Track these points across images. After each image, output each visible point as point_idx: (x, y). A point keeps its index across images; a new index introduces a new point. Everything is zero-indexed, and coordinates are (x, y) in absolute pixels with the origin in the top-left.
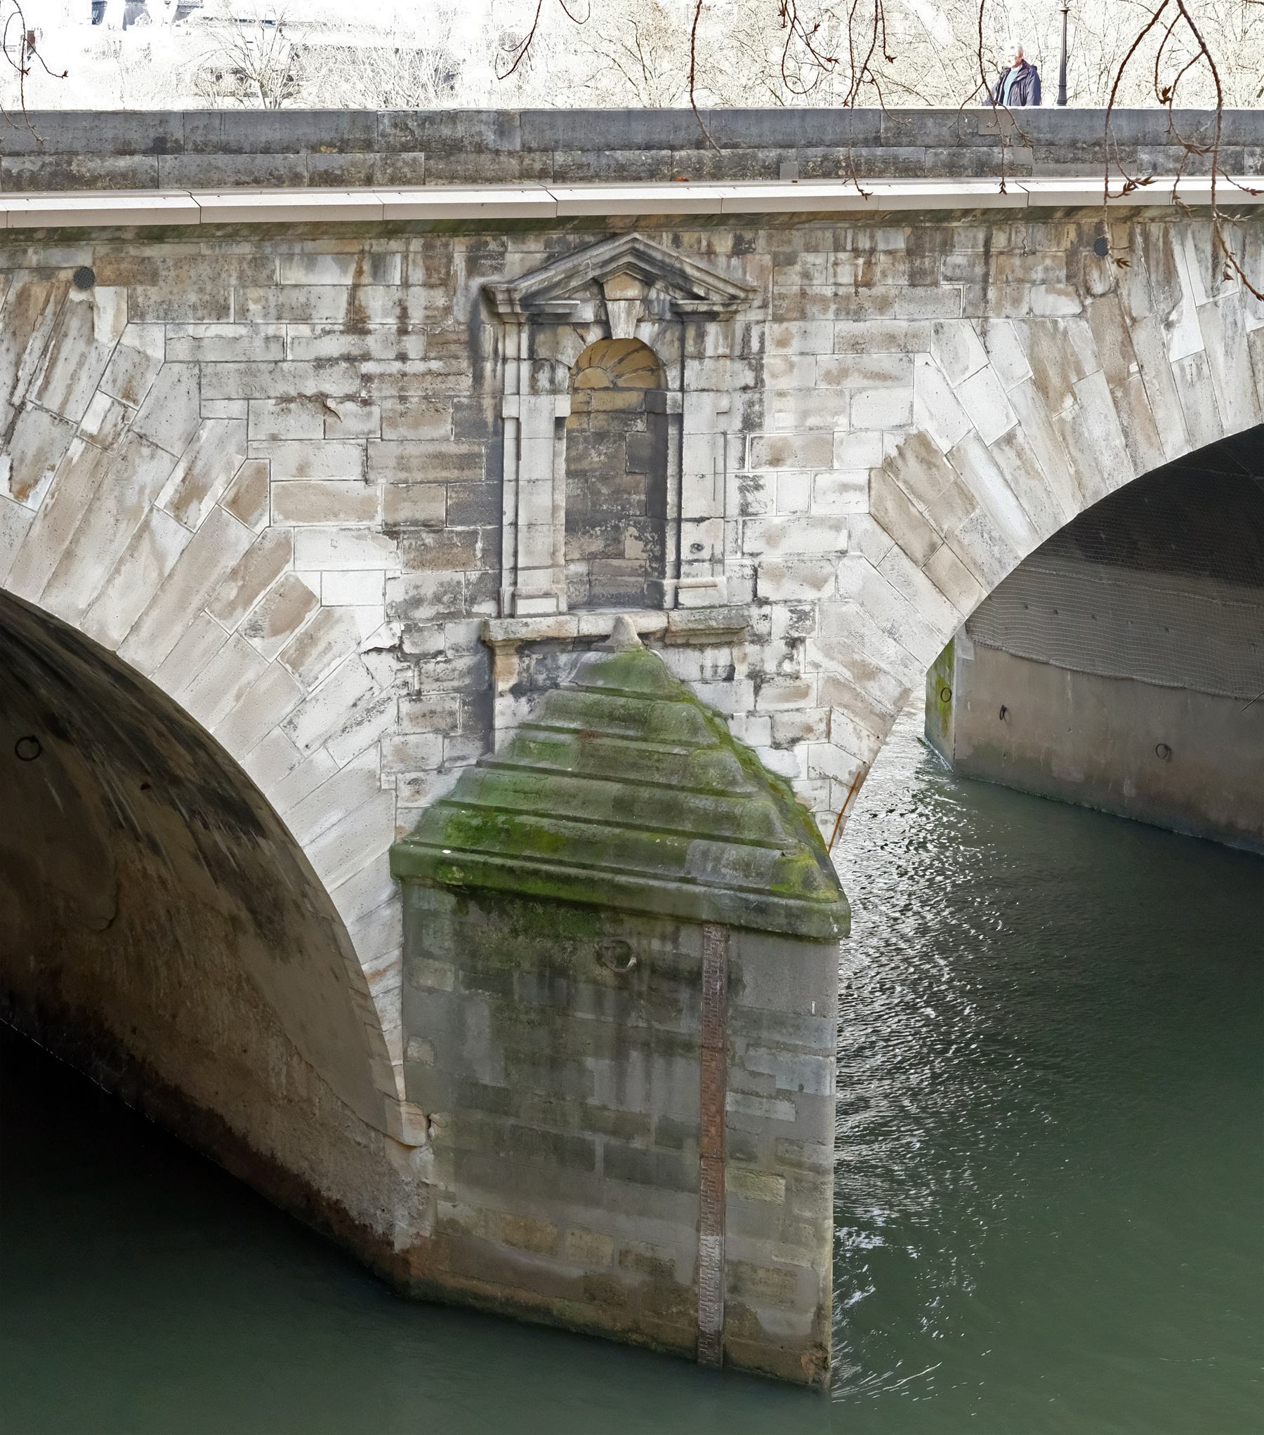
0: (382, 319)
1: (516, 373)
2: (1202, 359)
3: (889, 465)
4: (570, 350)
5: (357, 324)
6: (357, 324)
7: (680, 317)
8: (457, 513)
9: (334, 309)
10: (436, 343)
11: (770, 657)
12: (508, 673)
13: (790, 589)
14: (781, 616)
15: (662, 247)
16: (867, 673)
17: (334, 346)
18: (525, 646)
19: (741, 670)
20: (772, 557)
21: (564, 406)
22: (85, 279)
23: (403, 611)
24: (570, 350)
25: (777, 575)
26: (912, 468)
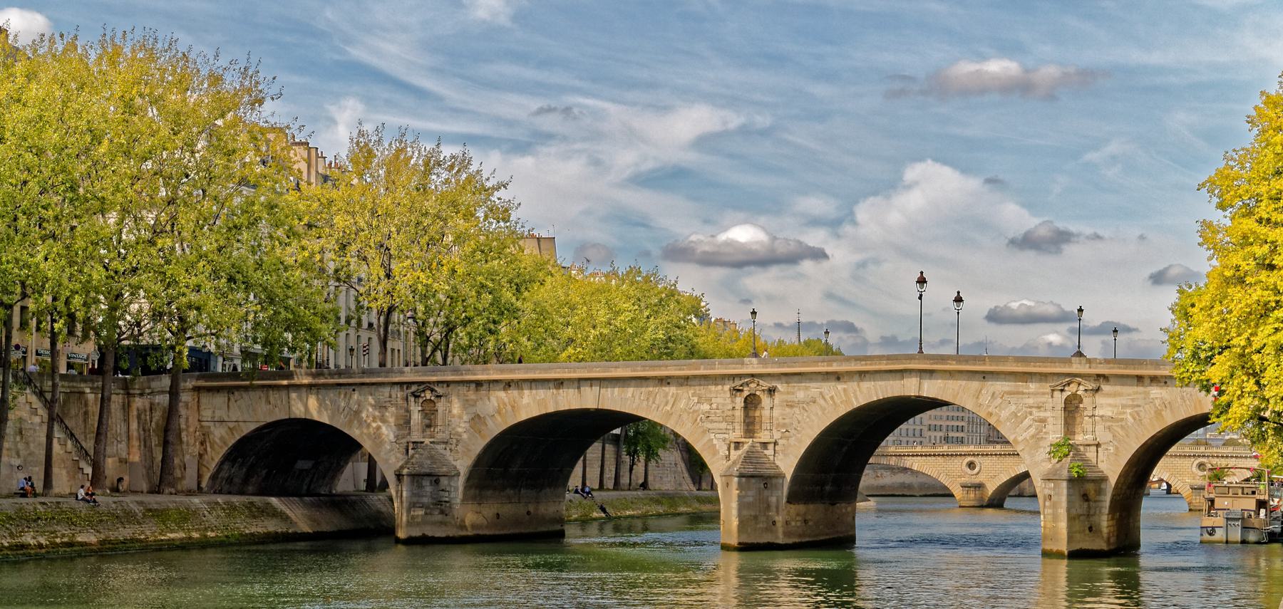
0: (394, 396)
1: (413, 404)
2: (528, 404)
3: (473, 419)
4: (421, 400)
5: (390, 397)
6: (390, 397)
7: (437, 396)
8: (405, 423)
9: (387, 394)
10: (402, 399)
11: (453, 447)
12: (411, 446)
13: (457, 437)
14: (455, 441)
15: (432, 386)
16: (469, 450)
17: (388, 399)
18: (413, 443)
19: (448, 449)
20: (453, 432)
21: (420, 408)
22: (354, 390)
23: (397, 437)
24: (421, 400)
25: (454, 435)
26: (476, 419)
